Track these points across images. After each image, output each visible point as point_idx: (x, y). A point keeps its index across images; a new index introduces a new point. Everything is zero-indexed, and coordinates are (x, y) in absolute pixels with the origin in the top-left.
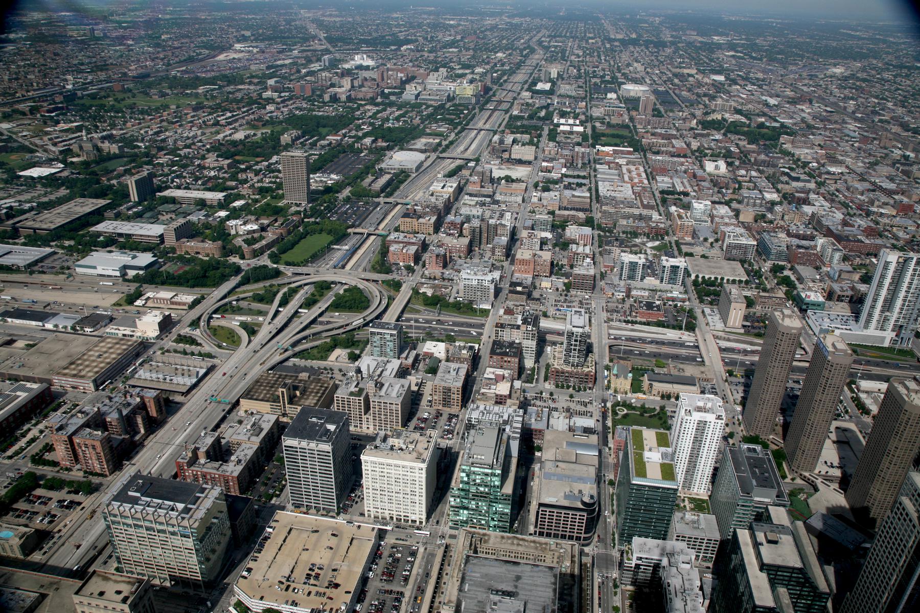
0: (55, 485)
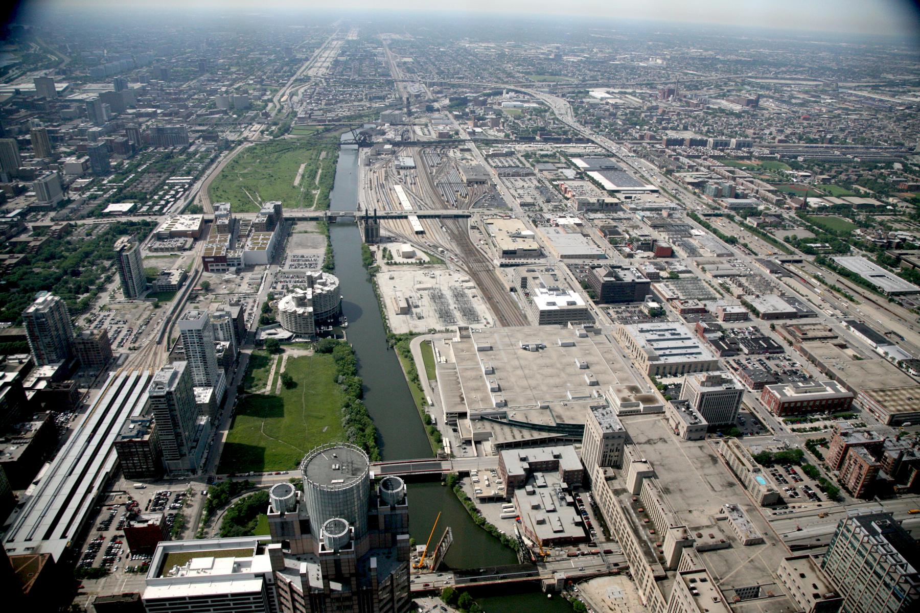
0: (811, 473)
